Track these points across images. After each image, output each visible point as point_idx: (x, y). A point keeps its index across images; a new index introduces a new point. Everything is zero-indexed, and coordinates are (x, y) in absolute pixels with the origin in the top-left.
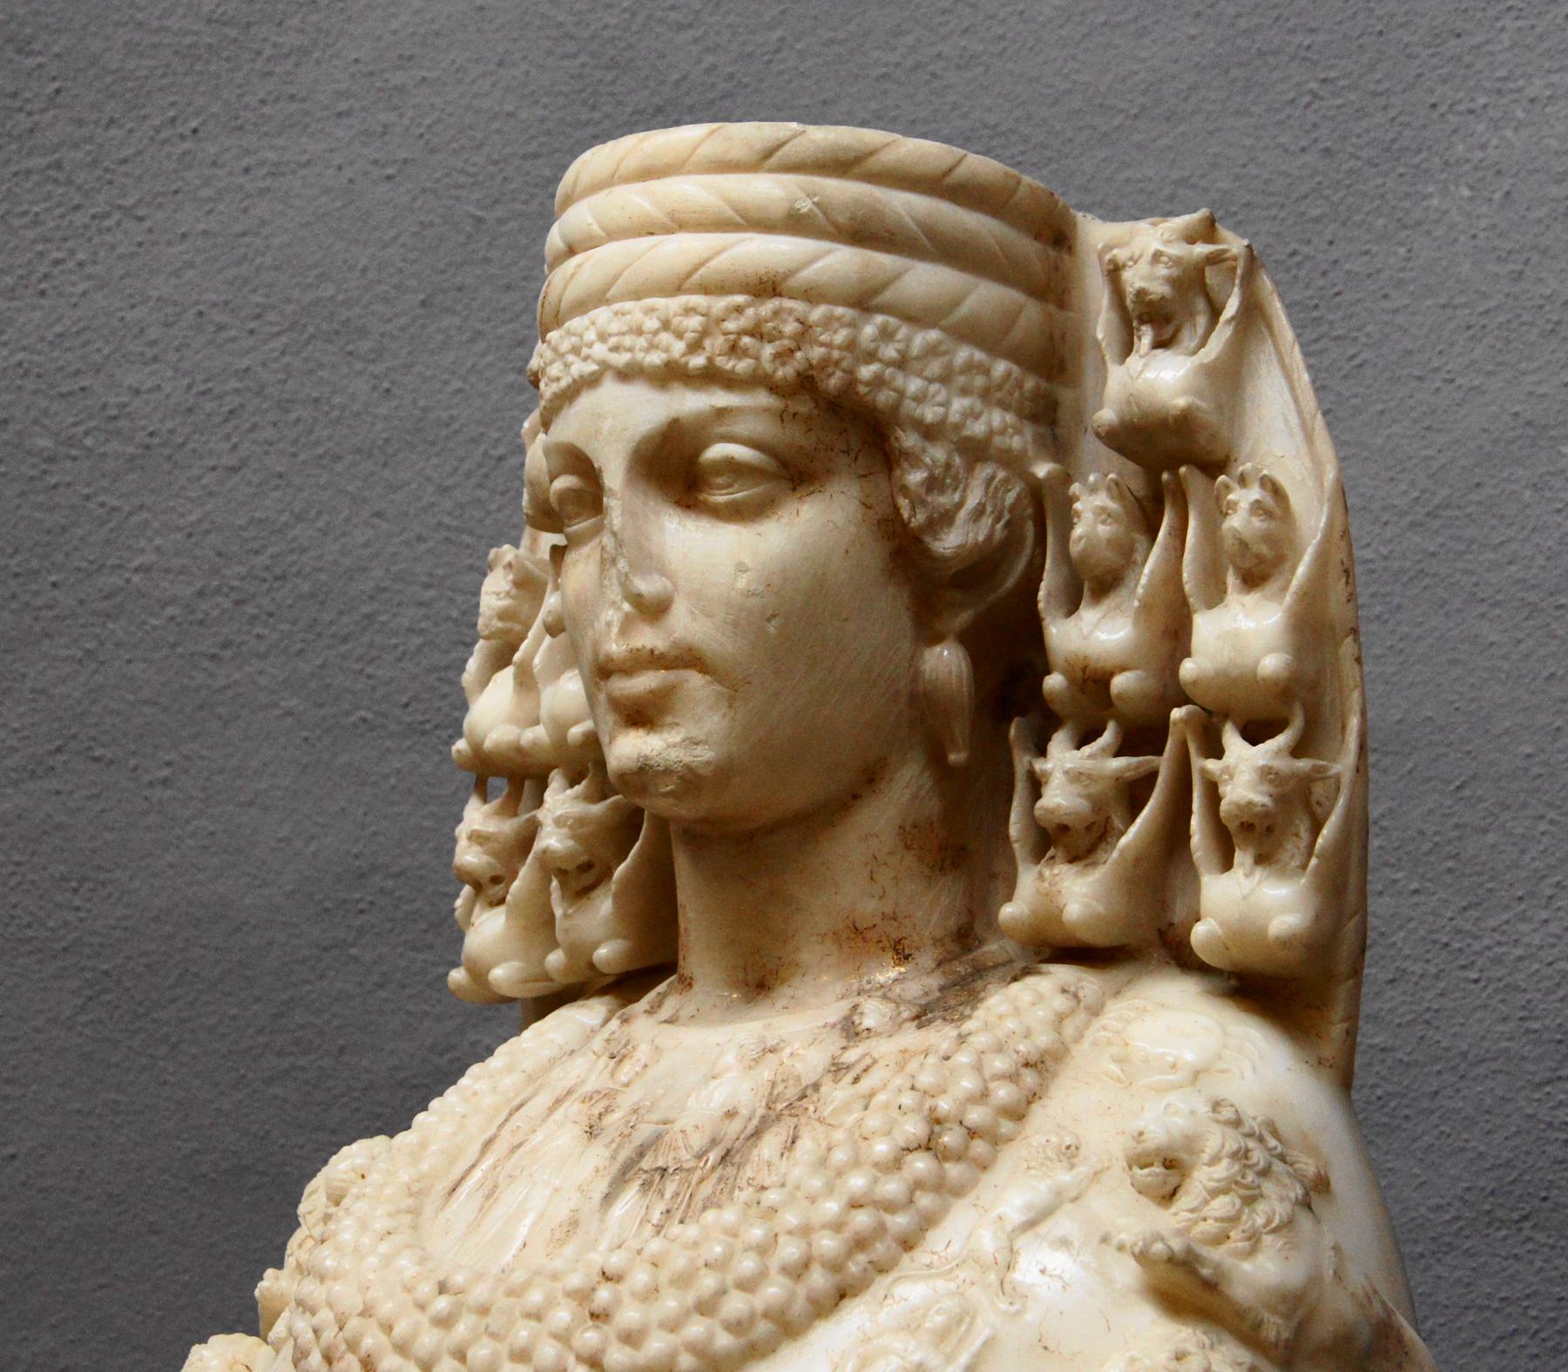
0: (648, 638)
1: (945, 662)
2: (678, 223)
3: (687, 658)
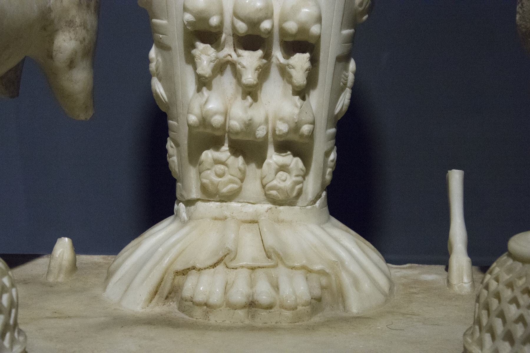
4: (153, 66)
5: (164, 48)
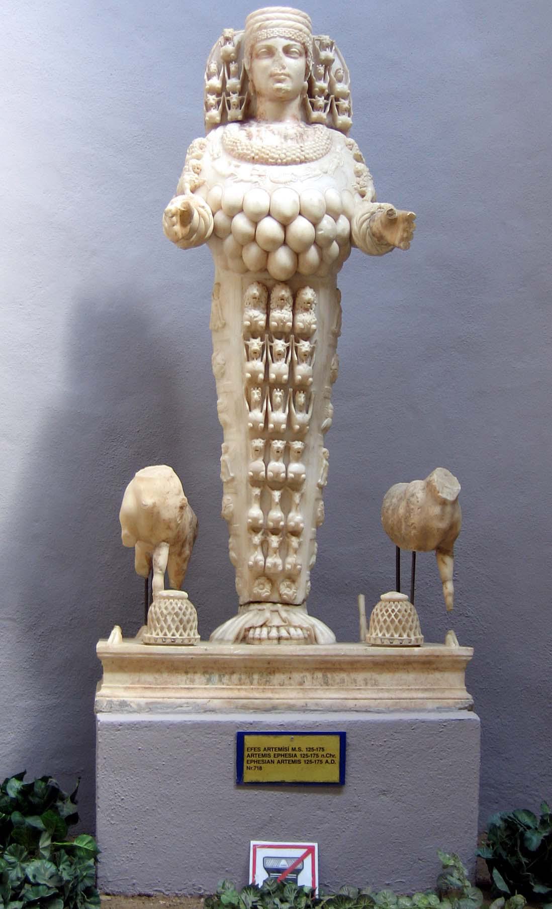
0: (282, 71)
1: (306, 83)
2: (289, 19)
3: (288, 76)
4: (230, 546)
5: (236, 535)
